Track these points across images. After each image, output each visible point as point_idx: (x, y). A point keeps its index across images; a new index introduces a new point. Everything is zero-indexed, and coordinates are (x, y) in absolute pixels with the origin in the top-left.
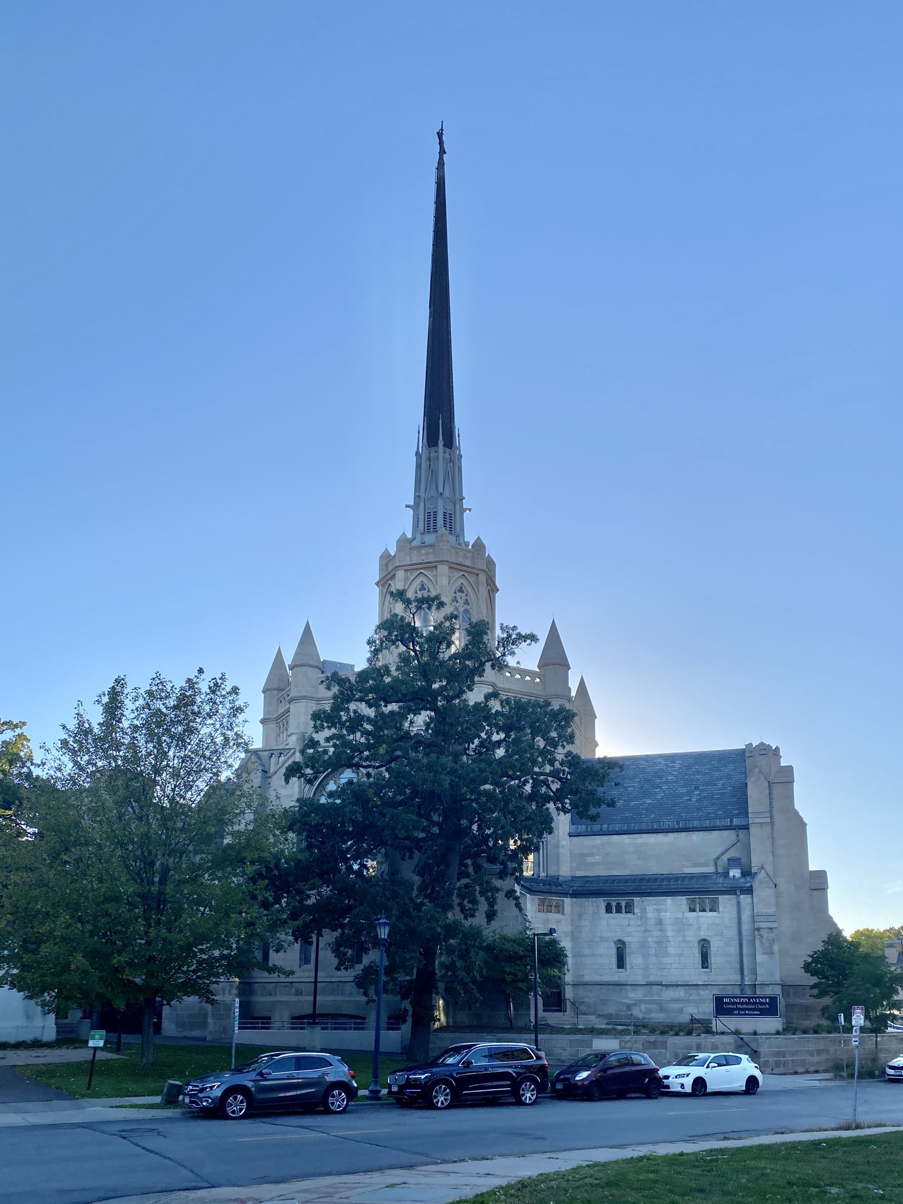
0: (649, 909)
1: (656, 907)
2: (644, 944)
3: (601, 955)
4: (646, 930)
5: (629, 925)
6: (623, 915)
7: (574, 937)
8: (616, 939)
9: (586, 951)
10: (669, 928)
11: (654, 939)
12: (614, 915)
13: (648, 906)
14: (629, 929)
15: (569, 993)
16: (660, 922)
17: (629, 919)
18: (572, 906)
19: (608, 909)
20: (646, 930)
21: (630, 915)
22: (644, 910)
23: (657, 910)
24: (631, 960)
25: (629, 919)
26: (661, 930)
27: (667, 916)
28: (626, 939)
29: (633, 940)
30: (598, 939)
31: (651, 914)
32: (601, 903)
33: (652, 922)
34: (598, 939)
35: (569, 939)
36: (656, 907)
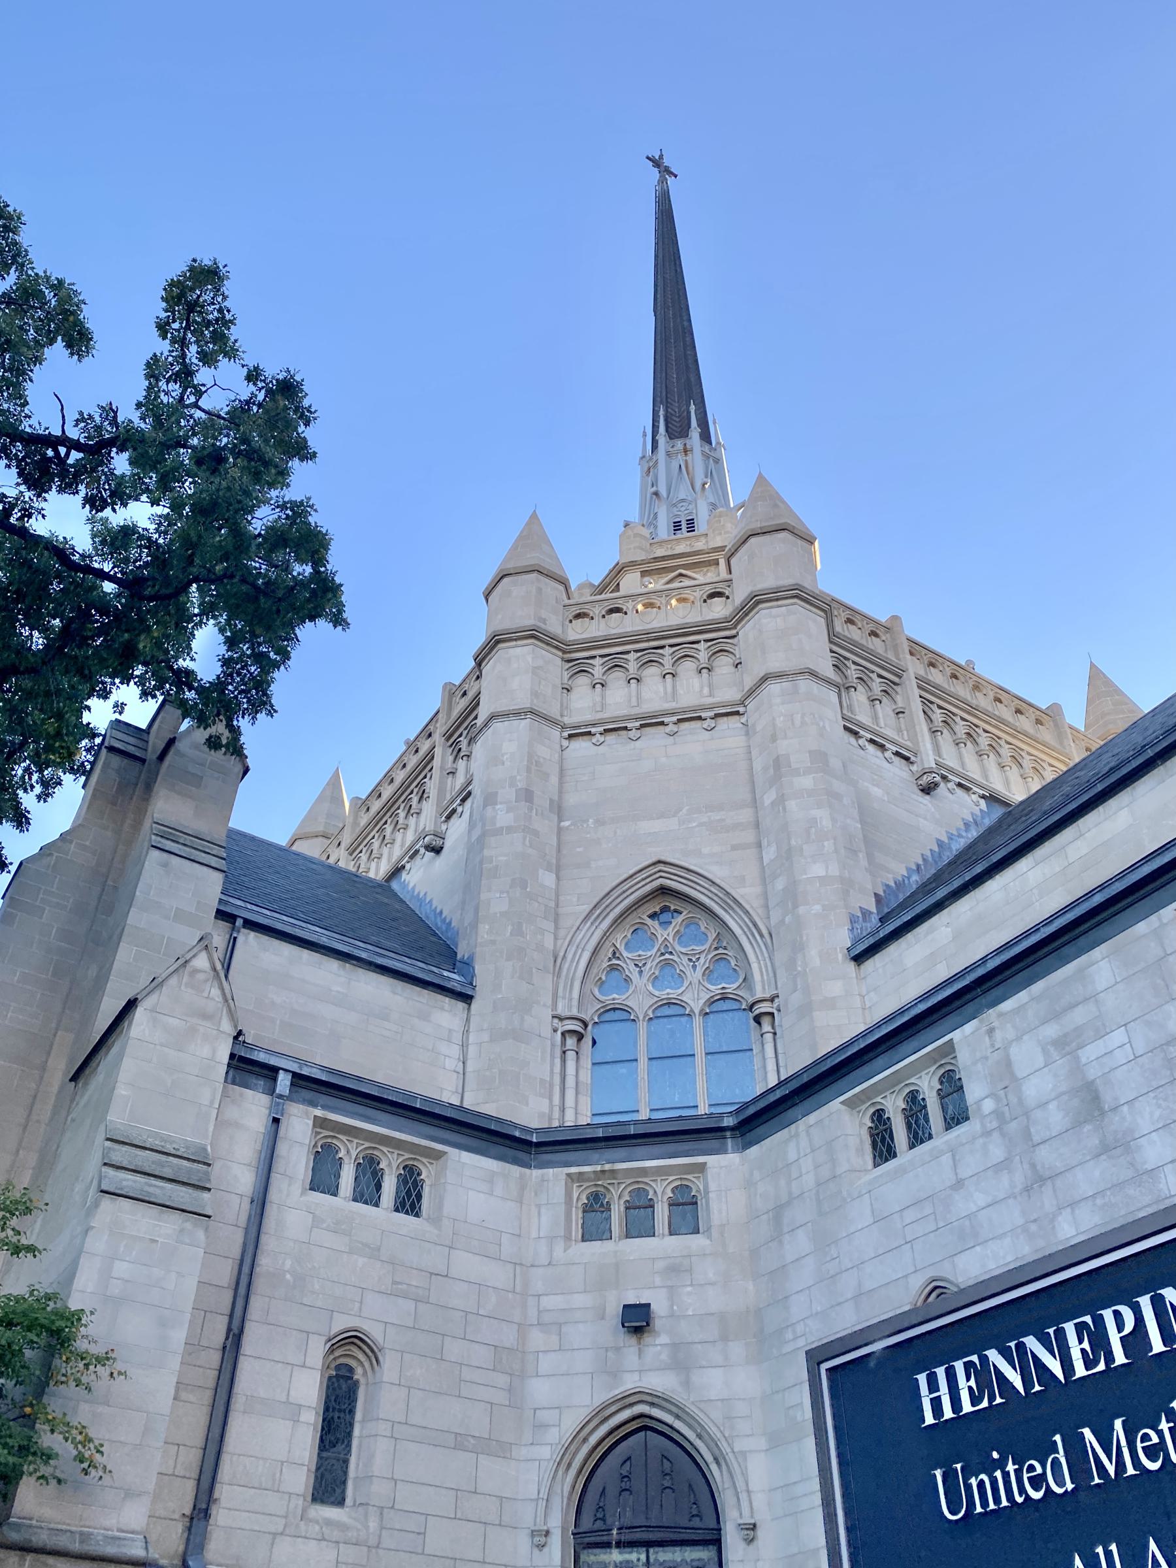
0: (1026, 1055)
1: (1051, 1031)
4: (1039, 1179)
5: (959, 1184)
14: (963, 1205)
16: (1090, 1102)
18: (749, 1184)
19: (883, 1148)
20: (1039, 1179)
22: (1006, 1077)
23: (1061, 1043)
26: (1105, 1149)
27: (1115, 1053)
31: (1041, 1083)
32: (838, 1122)
33: (1055, 1118)
35: (737, 1349)
36: (1051, 1031)
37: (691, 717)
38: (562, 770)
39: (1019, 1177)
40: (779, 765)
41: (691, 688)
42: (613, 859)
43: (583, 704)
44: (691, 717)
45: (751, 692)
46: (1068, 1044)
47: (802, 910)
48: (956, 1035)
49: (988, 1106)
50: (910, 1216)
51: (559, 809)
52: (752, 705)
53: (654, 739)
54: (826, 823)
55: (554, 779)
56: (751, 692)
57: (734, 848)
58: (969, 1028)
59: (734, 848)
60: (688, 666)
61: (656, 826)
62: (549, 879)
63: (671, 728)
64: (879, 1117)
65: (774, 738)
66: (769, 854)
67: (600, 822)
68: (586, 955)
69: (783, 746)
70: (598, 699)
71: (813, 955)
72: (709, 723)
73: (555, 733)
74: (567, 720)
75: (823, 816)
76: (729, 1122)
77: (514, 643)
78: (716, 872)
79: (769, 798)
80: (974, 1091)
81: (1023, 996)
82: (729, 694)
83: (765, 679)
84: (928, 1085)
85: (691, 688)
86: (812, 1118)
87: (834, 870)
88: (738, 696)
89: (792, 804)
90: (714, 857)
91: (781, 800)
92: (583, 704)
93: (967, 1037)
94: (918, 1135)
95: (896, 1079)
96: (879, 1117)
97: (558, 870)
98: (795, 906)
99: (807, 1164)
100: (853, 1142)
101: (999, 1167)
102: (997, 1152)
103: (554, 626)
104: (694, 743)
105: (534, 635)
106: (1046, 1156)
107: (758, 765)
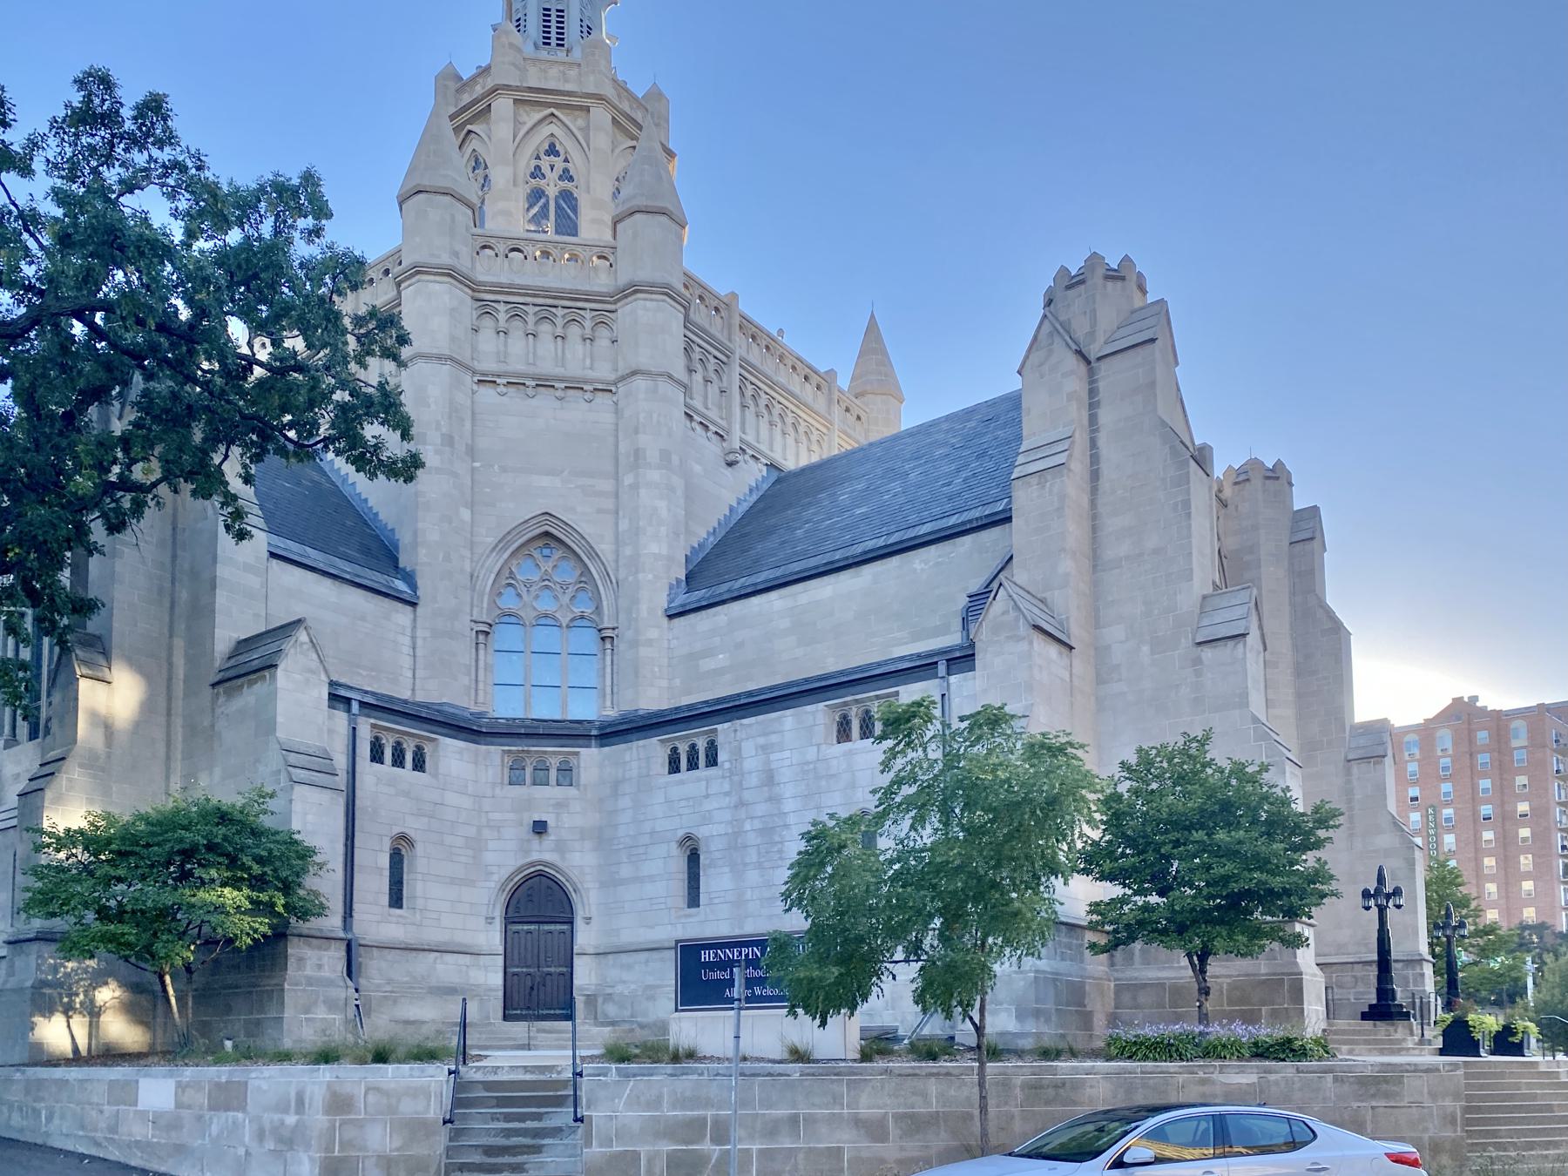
0: (748, 748)
1: (761, 740)
2: (735, 842)
3: (651, 879)
4: (741, 804)
5: (707, 796)
6: (703, 772)
7: (602, 839)
8: (681, 833)
9: (625, 871)
10: (788, 791)
11: (757, 824)
12: (685, 775)
13: (740, 739)
14: (709, 805)
15: (585, 975)
16: (770, 778)
17: (708, 780)
19: (674, 767)
20: (741, 804)
21: (713, 771)
22: (737, 753)
24: (714, 882)
25: (708, 780)
27: (785, 761)
28: (701, 832)
29: (712, 836)
30: (646, 839)
31: (751, 763)
32: (654, 749)
33: (753, 780)
34: (646, 839)
36: (761, 740)
37: (575, 386)
38: (473, 413)
39: (734, 799)
40: (638, 454)
41: (576, 358)
42: (517, 508)
43: (488, 350)
44: (575, 386)
45: (623, 378)
46: (765, 749)
47: (641, 576)
48: (719, 727)
49: (727, 765)
50: (683, 803)
51: (472, 452)
52: (622, 389)
53: (544, 402)
54: (664, 513)
55: (468, 425)
56: (623, 378)
57: (600, 511)
58: (726, 725)
59: (600, 511)
60: (574, 330)
61: (545, 481)
62: (466, 514)
63: (559, 393)
64: (674, 750)
65: (636, 432)
66: (624, 525)
67: (504, 470)
68: (493, 576)
69: (644, 440)
70: (502, 348)
71: (644, 607)
72: (588, 396)
73: (468, 379)
74: (478, 366)
75: (662, 505)
76: (594, 732)
77: (432, 278)
78: (585, 528)
79: (628, 480)
80: (722, 757)
81: (753, 720)
82: (604, 372)
83: (634, 373)
84: (702, 745)
85: (576, 358)
86: (641, 743)
87: (664, 552)
88: (612, 377)
89: (643, 492)
90: (586, 520)
91: (635, 487)
92: (488, 350)
93: (725, 731)
94: (693, 765)
95: (687, 736)
96: (674, 750)
97: (472, 506)
98: (637, 572)
99: (635, 764)
100: (660, 760)
101: (727, 794)
102: (727, 787)
103: (464, 264)
104: (576, 412)
105: (450, 273)
106: (747, 796)
107: (623, 448)
